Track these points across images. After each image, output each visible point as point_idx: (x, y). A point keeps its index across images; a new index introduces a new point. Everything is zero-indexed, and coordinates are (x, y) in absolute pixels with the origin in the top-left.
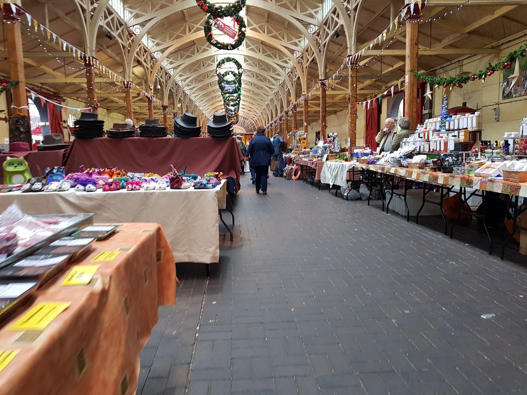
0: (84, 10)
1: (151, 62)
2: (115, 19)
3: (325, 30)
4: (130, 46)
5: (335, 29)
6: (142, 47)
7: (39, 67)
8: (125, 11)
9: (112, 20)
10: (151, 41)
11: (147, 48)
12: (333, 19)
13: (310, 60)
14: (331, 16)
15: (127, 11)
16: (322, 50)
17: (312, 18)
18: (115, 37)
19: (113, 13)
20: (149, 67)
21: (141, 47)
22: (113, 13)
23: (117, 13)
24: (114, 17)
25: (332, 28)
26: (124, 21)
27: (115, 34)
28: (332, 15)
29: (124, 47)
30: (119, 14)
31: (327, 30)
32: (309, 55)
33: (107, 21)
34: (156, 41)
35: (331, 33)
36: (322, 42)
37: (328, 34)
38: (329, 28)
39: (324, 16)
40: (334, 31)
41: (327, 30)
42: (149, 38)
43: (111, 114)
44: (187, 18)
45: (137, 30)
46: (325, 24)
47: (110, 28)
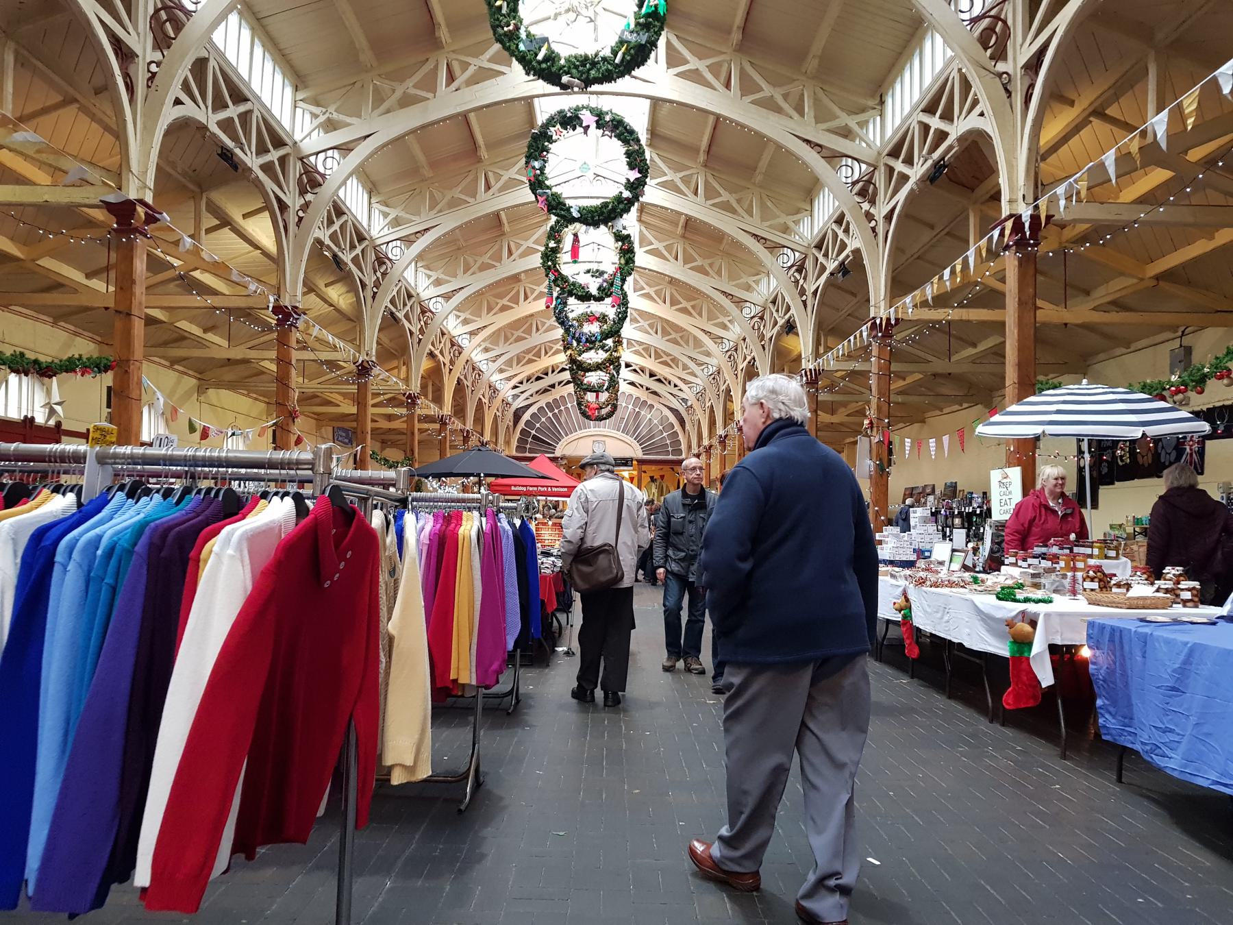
0: (125, 54)
1: (375, 272)
2: (256, 113)
3: (891, 170)
4: (306, 206)
5: (936, 155)
6: (350, 222)
7: (34, 260)
8: (299, 111)
9: (245, 117)
10: (381, 217)
11: (369, 234)
12: (926, 128)
13: (831, 266)
14: (920, 123)
15: (308, 117)
16: (881, 230)
17: (845, 137)
18: (250, 170)
19: (247, 100)
20: (370, 280)
21: (346, 221)
22: (247, 100)
23: (258, 98)
24: (250, 112)
25: (924, 152)
26: (291, 137)
27: (252, 161)
28: (926, 119)
29: (283, 207)
30: (276, 112)
31: (899, 166)
32: (826, 255)
33: (223, 115)
34: (393, 213)
35: (916, 172)
36: (881, 211)
37: (904, 178)
38: (909, 161)
39: (889, 133)
40: (930, 162)
41: (899, 166)
42: (375, 205)
43: (211, 392)
44: (483, 153)
45: (331, 166)
46: (894, 153)
47: (235, 138)
